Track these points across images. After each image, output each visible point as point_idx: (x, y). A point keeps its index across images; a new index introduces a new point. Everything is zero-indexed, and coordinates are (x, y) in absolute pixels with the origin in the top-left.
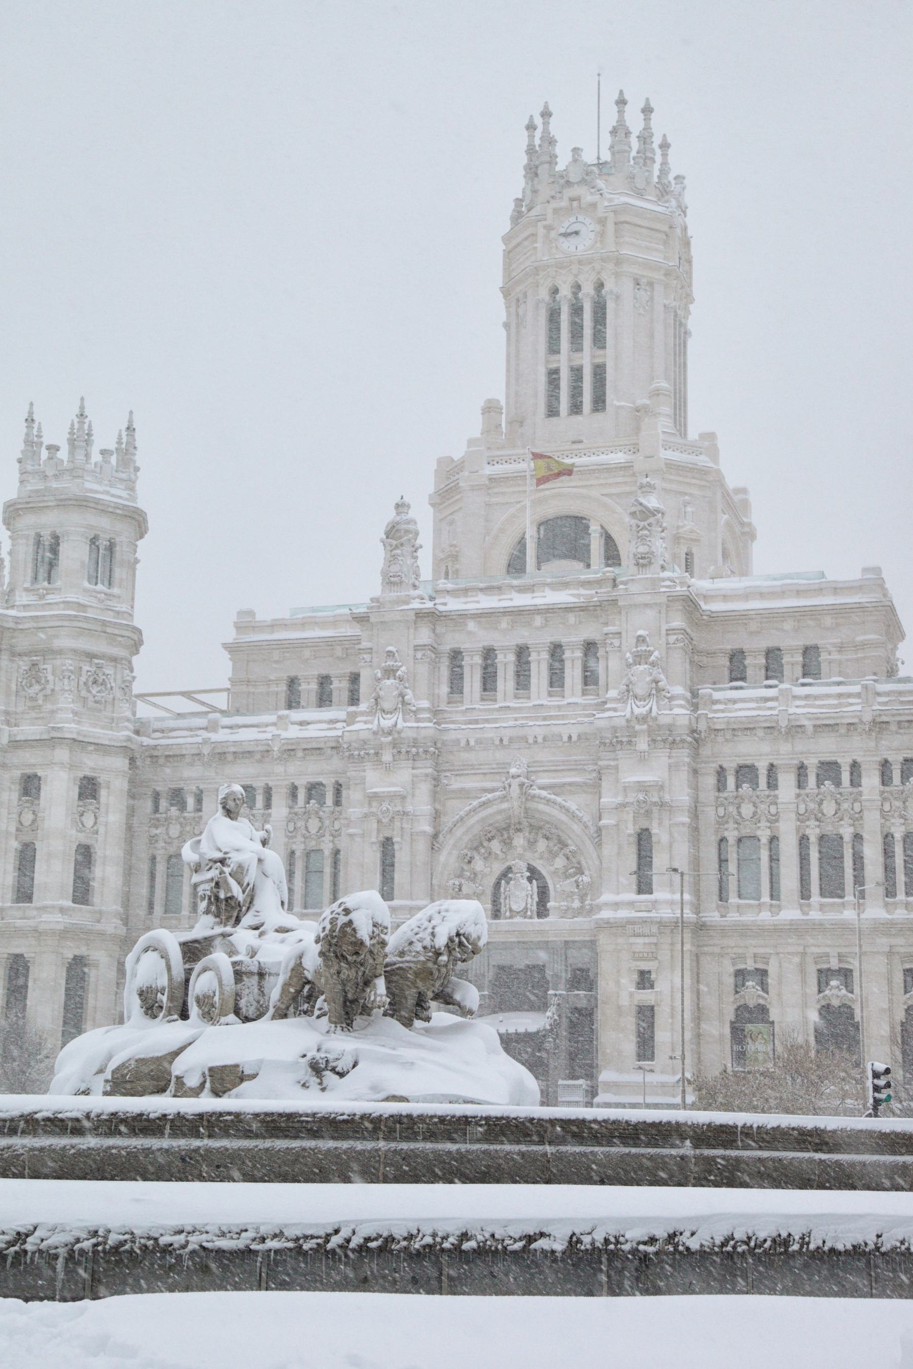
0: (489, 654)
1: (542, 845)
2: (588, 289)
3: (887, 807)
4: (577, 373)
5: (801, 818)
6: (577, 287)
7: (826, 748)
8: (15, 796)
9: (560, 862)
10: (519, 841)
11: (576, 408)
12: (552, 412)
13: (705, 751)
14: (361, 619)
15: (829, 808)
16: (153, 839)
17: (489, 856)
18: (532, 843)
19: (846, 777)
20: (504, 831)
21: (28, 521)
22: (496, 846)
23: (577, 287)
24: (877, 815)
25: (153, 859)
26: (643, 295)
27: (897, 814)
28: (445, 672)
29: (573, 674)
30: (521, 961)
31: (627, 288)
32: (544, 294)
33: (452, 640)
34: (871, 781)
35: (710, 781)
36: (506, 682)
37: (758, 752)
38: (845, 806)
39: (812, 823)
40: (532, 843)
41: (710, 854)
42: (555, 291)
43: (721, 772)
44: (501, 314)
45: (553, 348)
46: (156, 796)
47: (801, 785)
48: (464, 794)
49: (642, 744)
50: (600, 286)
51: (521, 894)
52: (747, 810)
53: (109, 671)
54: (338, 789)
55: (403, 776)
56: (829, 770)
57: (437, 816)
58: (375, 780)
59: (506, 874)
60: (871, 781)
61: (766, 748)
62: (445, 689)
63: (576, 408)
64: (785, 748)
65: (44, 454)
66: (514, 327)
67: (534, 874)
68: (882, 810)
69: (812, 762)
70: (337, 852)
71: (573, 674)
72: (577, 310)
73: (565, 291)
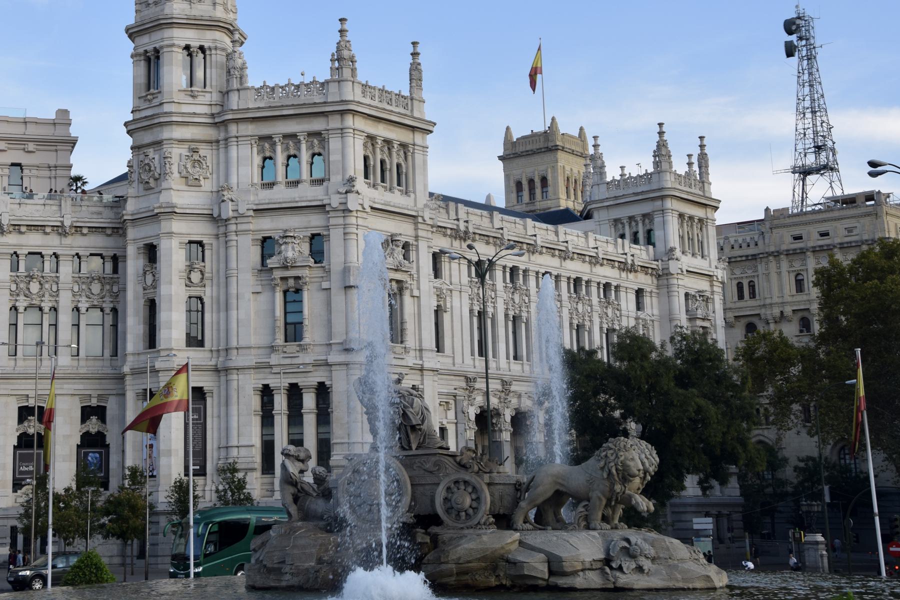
3: (76, 289)
24: (70, 294)
27: (83, 294)
34: (66, 269)
38: (47, 286)
39: (22, 298)
60: (66, 269)
68: (72, 290)
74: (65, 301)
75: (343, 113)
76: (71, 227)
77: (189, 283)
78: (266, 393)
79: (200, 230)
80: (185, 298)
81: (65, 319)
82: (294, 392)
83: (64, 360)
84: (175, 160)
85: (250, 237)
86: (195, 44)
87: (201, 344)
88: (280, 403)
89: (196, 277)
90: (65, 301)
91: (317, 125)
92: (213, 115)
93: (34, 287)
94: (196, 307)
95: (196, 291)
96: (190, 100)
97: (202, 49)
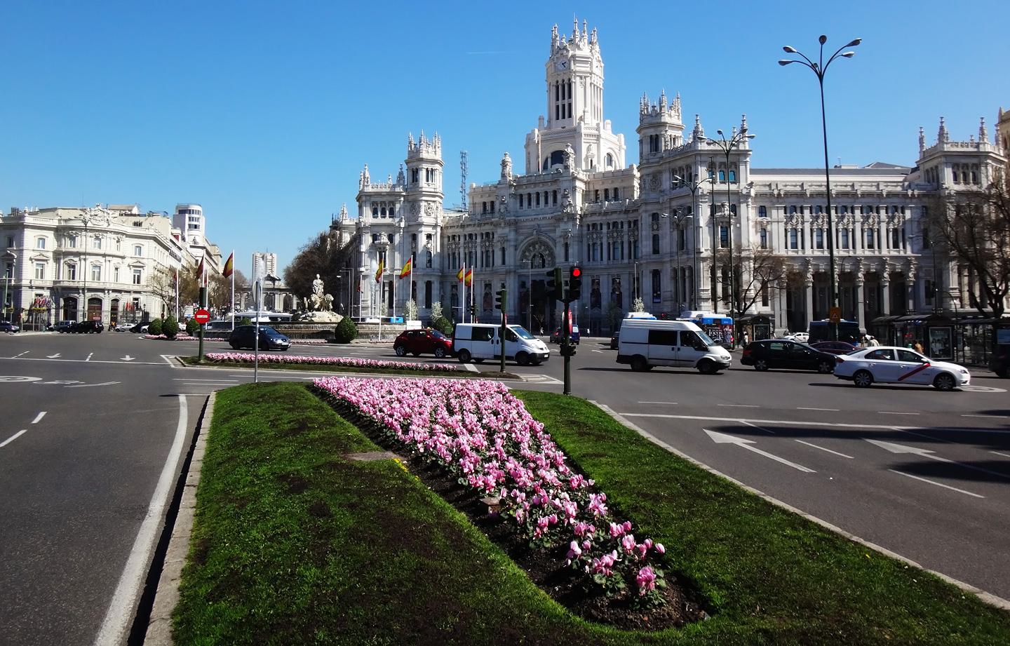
0: (529, 195)
1: (543, 248)
2: (566, 81)
4: (564, 106)
5: (608, 238)
6: (563, 81)
7: (614, 218)
8: (411, 240)
9: (547, 252)
10: (537, 246)
11: (564, 117)
12: (558, 118)
13: (584, 220)
14: (496, 187)
15: (615, 235)
16: (448, 249)
17: (529, 251)
18: (540, 247)
19: (620, 226)
20: (533, 244)
21: (411, 165)
22: (531, 248)
23: (563, 81)
25: (449, 254)
26: (583, 81)
28: (518, 201)
29: (551, 199)
30: (538, 278)
31: (578, 78)
32: (555, 84)
33: (520, 191)
34: (626, 227)
35: (585, 228)
36: (534, 203)
37: (596, 219)
40: (540, 247)
41: (585, 248)
42: (557, 82)
43: (588, 226)
44: (546, 88)
45: (558, 99)
46: (449, 237)
47: (609, 228)
48: (522, 234)
49: (566, 220)
50: (569, 80)
51: (538, 261)
52: (595, 236)
53: (432, 204)
54: (493, 234)
55: (507, 230)
56: (615, 224)
57: (516, 240)
58: (500, 231)
59: (534, 256)
60: (626, 227)
61: (599, 218)
62: (518, 205)
63: (564, 117)
64: (604, 218)
65: (413, 146)
66: (549, 91)
67: (542, 256)
69: (611, 222)
70: (493, 251)
71: (551, 199)
72: (563, 86)
73: (560, 82)
74: (626, 238)
75: (696, 155)
76: (626, 211)
77: (653, 230)
78: (675, 271)
79: (653, 209)
80: (651, 235)
81: (626, 246)
82: (683, 270)
83: (626, 261)
84: (647, 181)
85: (707, 204)
86: (654, 134)
87: (658, 253)
88: (679, 274)
89: (655, 227)
90: (626, 238)
91: (689, 161)
92: (658, 162)
93: (615, 235)
94: (656, 239)
95: (655, 233)
96: (652, 157)
97: (657, 135)
